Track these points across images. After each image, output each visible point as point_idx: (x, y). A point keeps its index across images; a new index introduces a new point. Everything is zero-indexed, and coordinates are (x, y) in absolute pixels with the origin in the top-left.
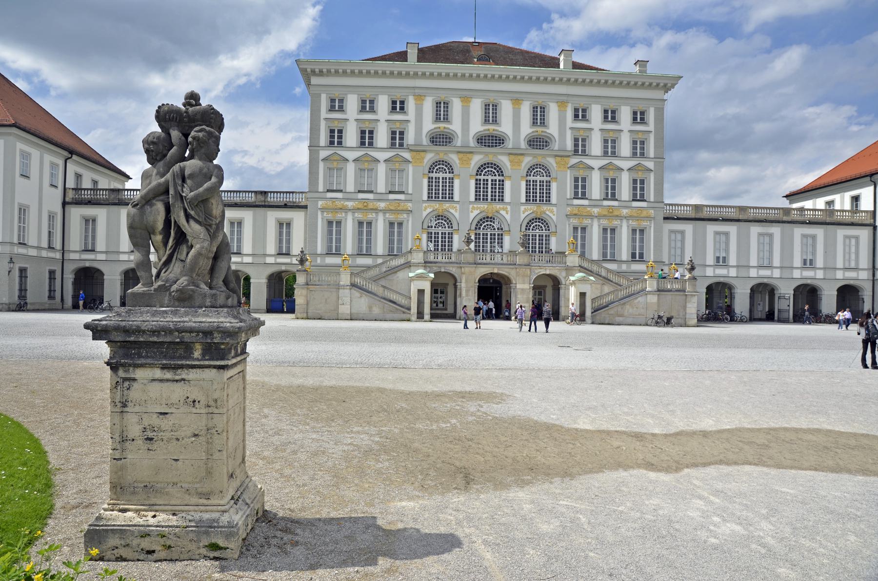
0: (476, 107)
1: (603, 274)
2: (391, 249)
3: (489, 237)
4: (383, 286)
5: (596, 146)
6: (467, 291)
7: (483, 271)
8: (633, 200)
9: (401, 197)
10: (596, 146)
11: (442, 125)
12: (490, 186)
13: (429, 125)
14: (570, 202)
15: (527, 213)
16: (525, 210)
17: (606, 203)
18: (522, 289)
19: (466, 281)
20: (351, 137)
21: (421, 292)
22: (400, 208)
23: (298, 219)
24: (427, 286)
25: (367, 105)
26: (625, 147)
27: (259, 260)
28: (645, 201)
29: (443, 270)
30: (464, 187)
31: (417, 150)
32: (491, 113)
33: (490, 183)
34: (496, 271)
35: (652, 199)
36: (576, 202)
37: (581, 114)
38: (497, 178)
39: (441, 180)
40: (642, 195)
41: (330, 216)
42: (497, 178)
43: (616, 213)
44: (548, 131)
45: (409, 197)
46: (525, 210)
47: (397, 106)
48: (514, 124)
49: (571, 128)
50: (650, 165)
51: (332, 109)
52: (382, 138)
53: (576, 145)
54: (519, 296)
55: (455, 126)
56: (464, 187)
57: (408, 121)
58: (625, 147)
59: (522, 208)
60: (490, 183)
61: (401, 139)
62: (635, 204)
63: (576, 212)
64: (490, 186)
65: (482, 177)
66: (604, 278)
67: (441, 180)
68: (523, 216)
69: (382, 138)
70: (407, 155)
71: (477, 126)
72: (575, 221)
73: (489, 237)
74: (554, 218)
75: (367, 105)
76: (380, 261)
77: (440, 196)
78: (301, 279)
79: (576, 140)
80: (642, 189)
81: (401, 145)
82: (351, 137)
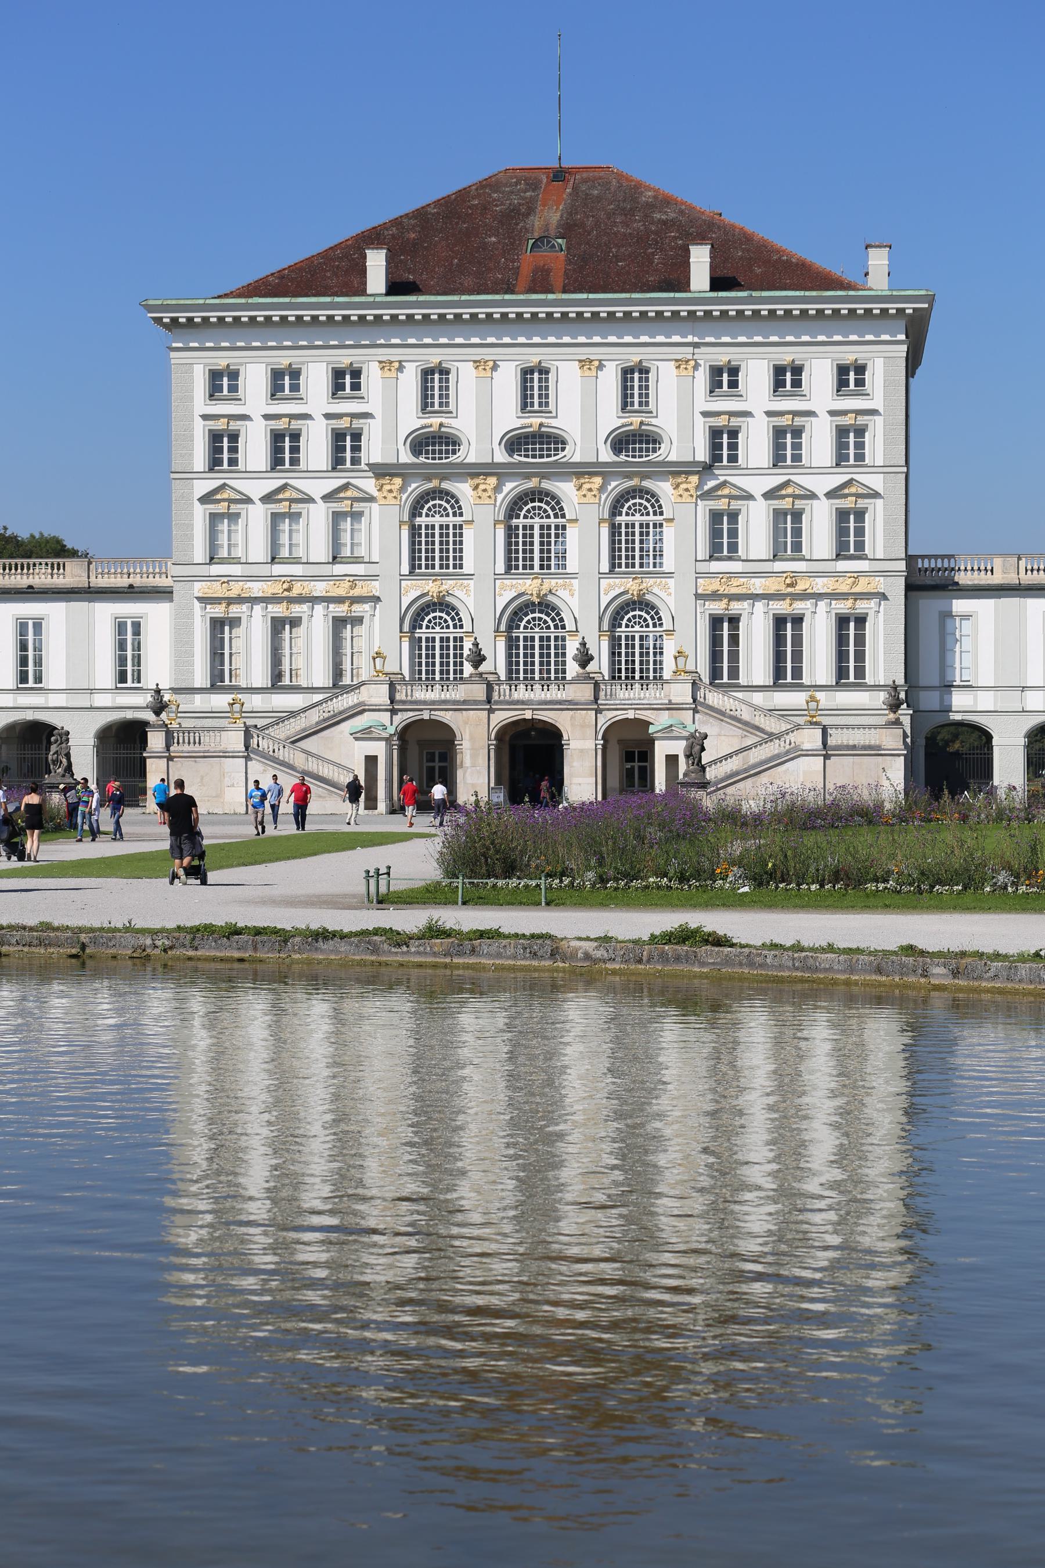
0: (508, 378)
1: (746, 715)
2: (338, 673)
3: (537, 643)
4: (304, 751)
5: (756, 444)
6: (474, 757)
7: (501, 717)
8: (839, 557)
9: (359, 569)
10: (756, 444)
11: (435, 421)
12: (537, 540)
13: (411, 419)
14: (702, 567)
15: (613, 594)
16: (611, 587)
17: (779, 566)
18: (582, 751)
19: (472, 738)
20: (255, 449)
21: (371, 761)
22: (356, 592)
23: (156, 616)
24: (378, 749)
25: (284, 381)
26: (819, 443)
27: (83, 701)
28: (865, 558)
29: (426, 716)
30: (482, 543)
31: (382, 472)
32: (533, 385)
33: (537, 532)
34: (528, 715)
35: (880, 555)
36: (716, 566)
37: (725, 378)
38: (552, 521)
39: (437, 531)
40: (860, 546)
41: (218, 611)
42: (552, 521)
43: (801, 587)
44: (654, 421)
45: (372, 570)
46: (611, 587)
47: (345, 380)
48: (584, 408)
49: (705, 414)
50: (875, 482)
51: (214, 391)
52: (316, 448)
53: (715, 447)
54: (575, 764)
55: (464, 422)
56: (482, 543)
57: (367, 415)
58: (819, 443)
59: (604, 583)
60: (537, 532)
61: (356, 449)
62: (843, 565)
63: (714, 585)
64: (537, 540)
65: (520, 522)
66: (746, 723)
67: (437, 531)
68: (605, 600)
69: (316, 448)
70: (369, 485)
71: (509, 417)
72: (717, 607)
73: (537, 643)
74: (671, 601)
75: (284, 381)
76: (318, 697)
77: (437, 562)
78: (156, 741)
79: (715, 433)
80: (860, 532)
81: (355, 461)
82: (255, 449)
